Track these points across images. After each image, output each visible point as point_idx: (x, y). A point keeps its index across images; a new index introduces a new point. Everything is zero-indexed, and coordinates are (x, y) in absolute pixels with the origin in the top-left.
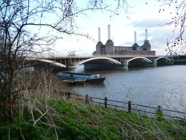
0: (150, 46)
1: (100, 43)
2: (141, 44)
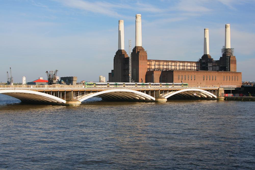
0: (235, 62)
1: (120, 55)
2: (216, 56)
